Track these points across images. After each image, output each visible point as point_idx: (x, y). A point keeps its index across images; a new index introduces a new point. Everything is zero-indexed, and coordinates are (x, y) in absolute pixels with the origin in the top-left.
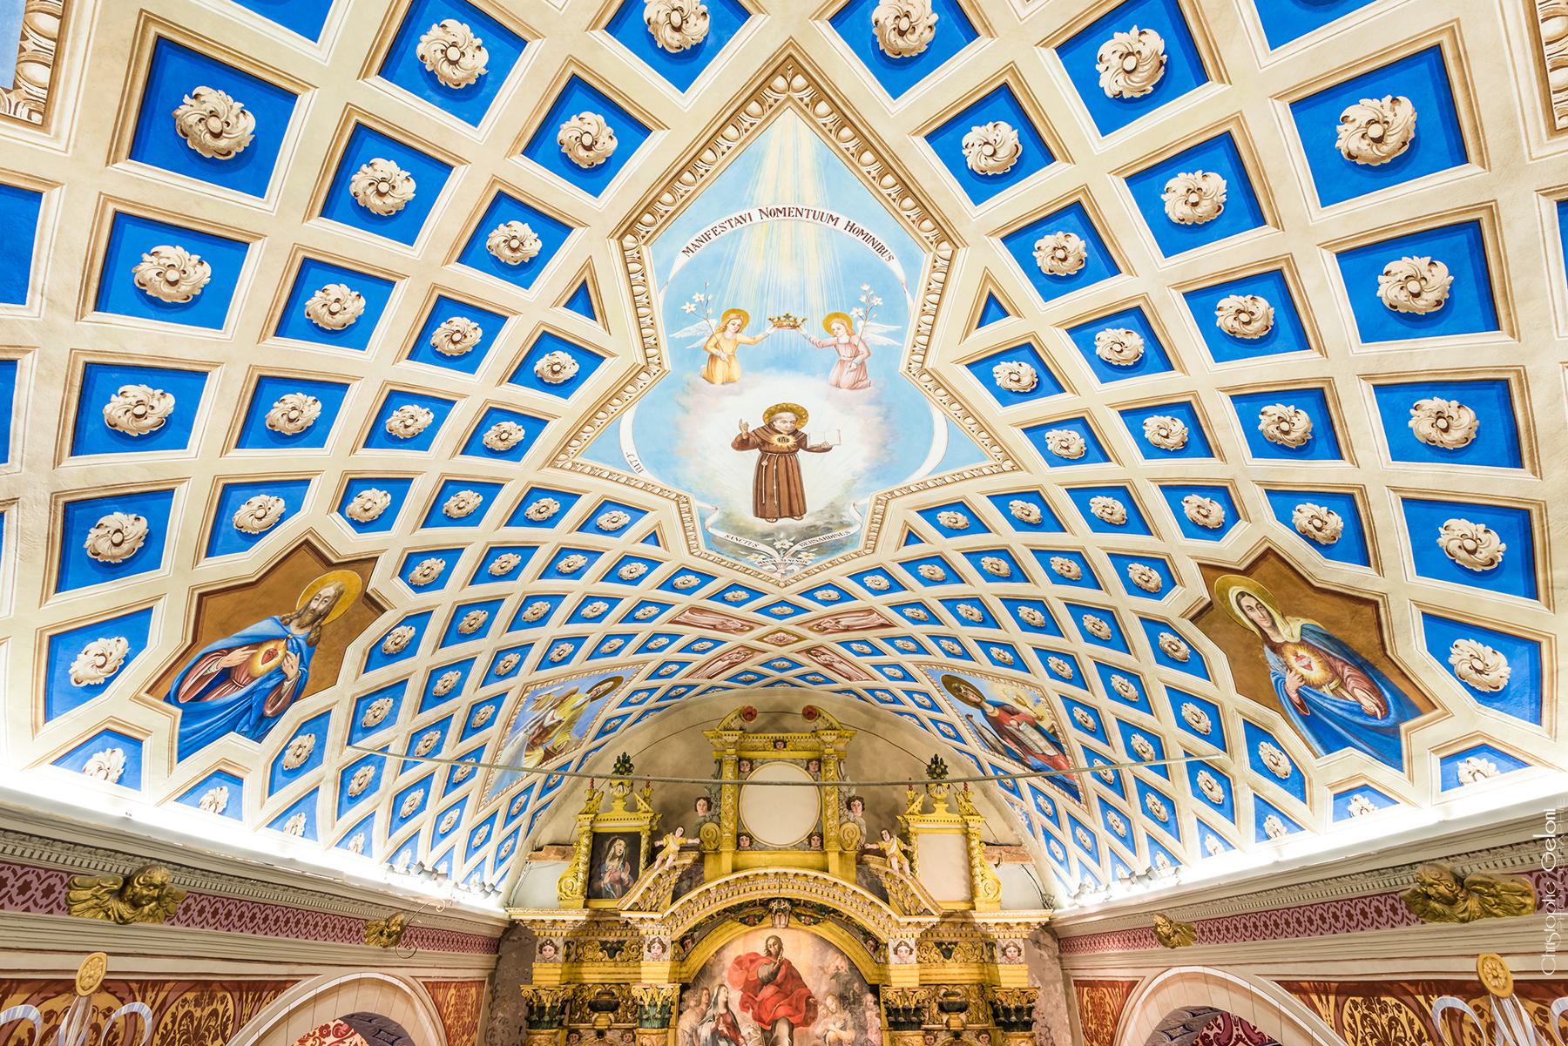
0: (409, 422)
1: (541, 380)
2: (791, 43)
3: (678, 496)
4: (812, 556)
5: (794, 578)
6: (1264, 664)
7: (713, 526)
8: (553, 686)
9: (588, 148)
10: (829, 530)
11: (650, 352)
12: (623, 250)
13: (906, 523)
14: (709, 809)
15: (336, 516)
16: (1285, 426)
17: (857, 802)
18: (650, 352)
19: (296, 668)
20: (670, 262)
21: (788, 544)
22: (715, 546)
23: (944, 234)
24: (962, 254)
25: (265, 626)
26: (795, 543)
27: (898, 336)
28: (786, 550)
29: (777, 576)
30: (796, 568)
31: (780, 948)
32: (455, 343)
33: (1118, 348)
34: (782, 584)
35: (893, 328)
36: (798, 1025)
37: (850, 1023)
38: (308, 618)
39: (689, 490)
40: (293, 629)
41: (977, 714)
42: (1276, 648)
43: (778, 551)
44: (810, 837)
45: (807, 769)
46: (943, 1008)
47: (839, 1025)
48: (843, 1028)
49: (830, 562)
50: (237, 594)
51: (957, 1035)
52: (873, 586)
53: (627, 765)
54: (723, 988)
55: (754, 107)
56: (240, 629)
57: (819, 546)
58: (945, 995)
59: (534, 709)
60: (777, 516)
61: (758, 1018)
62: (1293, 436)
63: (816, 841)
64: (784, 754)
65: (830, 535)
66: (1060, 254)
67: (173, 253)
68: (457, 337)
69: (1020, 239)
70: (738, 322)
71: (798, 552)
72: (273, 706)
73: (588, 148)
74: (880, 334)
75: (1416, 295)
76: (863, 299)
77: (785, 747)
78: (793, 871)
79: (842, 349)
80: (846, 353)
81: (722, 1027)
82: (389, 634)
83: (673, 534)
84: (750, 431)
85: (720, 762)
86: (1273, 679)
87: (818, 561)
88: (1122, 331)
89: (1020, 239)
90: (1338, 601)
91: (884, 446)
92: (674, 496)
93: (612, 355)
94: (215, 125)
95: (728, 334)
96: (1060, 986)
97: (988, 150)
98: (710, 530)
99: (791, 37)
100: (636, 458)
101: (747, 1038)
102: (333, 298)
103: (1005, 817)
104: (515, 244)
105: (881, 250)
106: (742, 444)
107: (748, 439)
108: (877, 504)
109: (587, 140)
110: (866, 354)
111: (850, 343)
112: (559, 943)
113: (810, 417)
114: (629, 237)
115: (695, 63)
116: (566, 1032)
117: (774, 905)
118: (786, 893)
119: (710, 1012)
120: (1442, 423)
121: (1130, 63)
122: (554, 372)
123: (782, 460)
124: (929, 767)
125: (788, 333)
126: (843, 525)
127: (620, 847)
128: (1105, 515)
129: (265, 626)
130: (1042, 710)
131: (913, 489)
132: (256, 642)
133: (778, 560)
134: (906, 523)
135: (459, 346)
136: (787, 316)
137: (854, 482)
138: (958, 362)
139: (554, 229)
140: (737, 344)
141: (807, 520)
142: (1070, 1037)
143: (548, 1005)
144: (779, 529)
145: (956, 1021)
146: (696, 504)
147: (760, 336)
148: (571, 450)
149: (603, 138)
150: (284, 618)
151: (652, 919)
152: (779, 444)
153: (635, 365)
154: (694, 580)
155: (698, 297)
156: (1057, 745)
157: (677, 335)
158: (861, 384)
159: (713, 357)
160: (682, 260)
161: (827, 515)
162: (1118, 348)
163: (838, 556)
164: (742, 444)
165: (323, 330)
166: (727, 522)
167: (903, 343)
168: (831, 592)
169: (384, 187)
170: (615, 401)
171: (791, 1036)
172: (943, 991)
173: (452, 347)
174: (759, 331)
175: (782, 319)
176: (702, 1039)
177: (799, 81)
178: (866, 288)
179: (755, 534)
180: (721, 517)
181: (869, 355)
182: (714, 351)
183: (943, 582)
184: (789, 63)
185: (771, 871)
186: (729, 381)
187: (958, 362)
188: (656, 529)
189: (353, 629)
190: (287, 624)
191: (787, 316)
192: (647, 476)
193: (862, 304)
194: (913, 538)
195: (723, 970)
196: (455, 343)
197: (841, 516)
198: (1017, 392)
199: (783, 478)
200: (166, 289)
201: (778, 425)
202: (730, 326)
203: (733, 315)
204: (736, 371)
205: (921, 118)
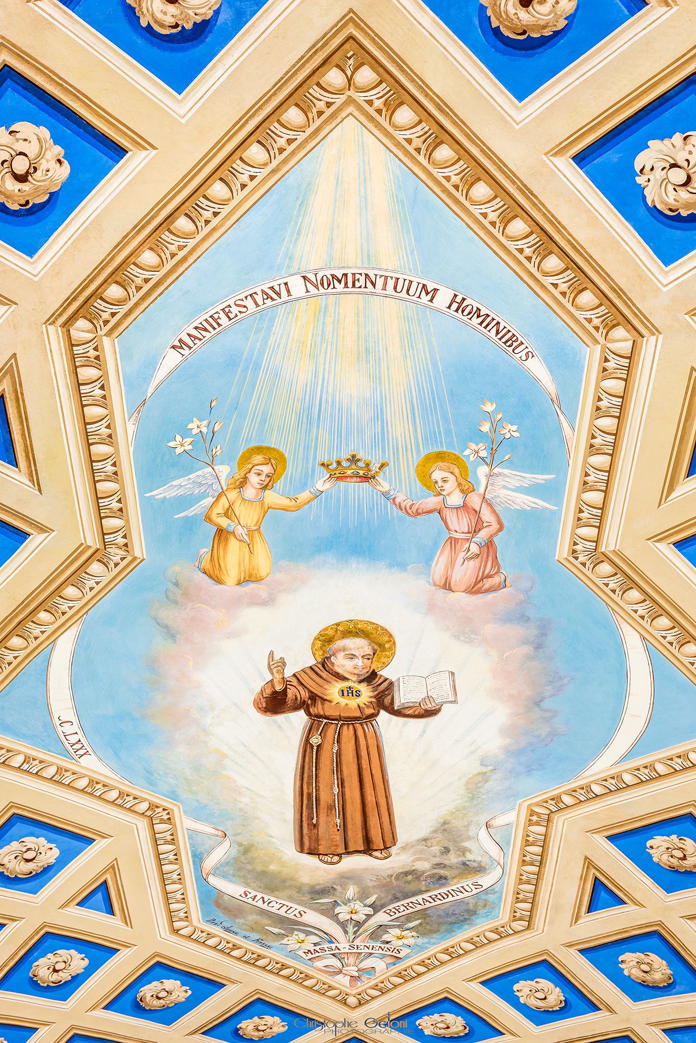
2: (351, 17)
3: (153, 807)
4: (410, 939)
5: (375, 987)
9: (22, 178)
10: (441, 880)
11: (111, 523)
13: (589, 863)
18: (111, 523)
20: (152, 364)
21: (362, 911)
22: (220, 916)
24: (650, 346)
27: (551, 491)
28: (359, 924)
29: (342, 981)
30: (380, 965)
34: (352, 1001)
35: (540, 478)
39: (174, 796)
43: (343, 925)
49: (446, 951)
52: (533, 1002)
55: (293, 115)
60: (341, 850)
65: (443, 890)
70: (267, 469)
73: (22, 178)
74: (518, 490)
76: (486, 428)
79: (452, 518)
80: (460, 524)
84: (288, 673)
87: (422, 948)
91: (537, 704)
92: (143, 807)
93: (42, 529)
95: (250, 492)
98: (212, 880)
99: (351, 11)
100: (75, 728)
105: (511, 341)
107: (285, 690)
108: (530, 823)
109: (20, 166)
110: (495, 526)
111: (465, 506)
114: (82, 323)
115: (199, 50)
123: (348, 733)
125: (354, 488)
126: (469, 869)
131: (597, 789)
133: (344, 946)
134: (589, 863)
136: (354, 459)
137: (484, 777)
138: (659, 538)
140: (266, 510)
144: (346, 878)
146: (185, 823)
147: (304, 496)
149: (48, 163)
152: (343, 701)
153: (81, 548)
154: (178, 991)
157: (159, 493)
158: (488, 583)
159: (221, 534)
160: (173, 359)
161: (436, 849)
163: (461, 936)
167: (559, 504)
168: (450, 1018)
170: (43, 616)
174: (304, 486)
175: (345, 464)
178: (489, 407)
179: (299, 889)
180: (234, 852)
181: (501, 527)
182: (224, 522)
183: (667, 989)
186: (249, 578)
187: (659, 538)
188: (108, 877)
191: (354, 459)
192: (92, 764)
193: (482, 436)
194: (603, 894)
197: (464, 851)
199: (350, 770)
201: (341, 663)
202: (254, 479)
203: (258, 459)
204: (263, 561)
205: (563, 128)
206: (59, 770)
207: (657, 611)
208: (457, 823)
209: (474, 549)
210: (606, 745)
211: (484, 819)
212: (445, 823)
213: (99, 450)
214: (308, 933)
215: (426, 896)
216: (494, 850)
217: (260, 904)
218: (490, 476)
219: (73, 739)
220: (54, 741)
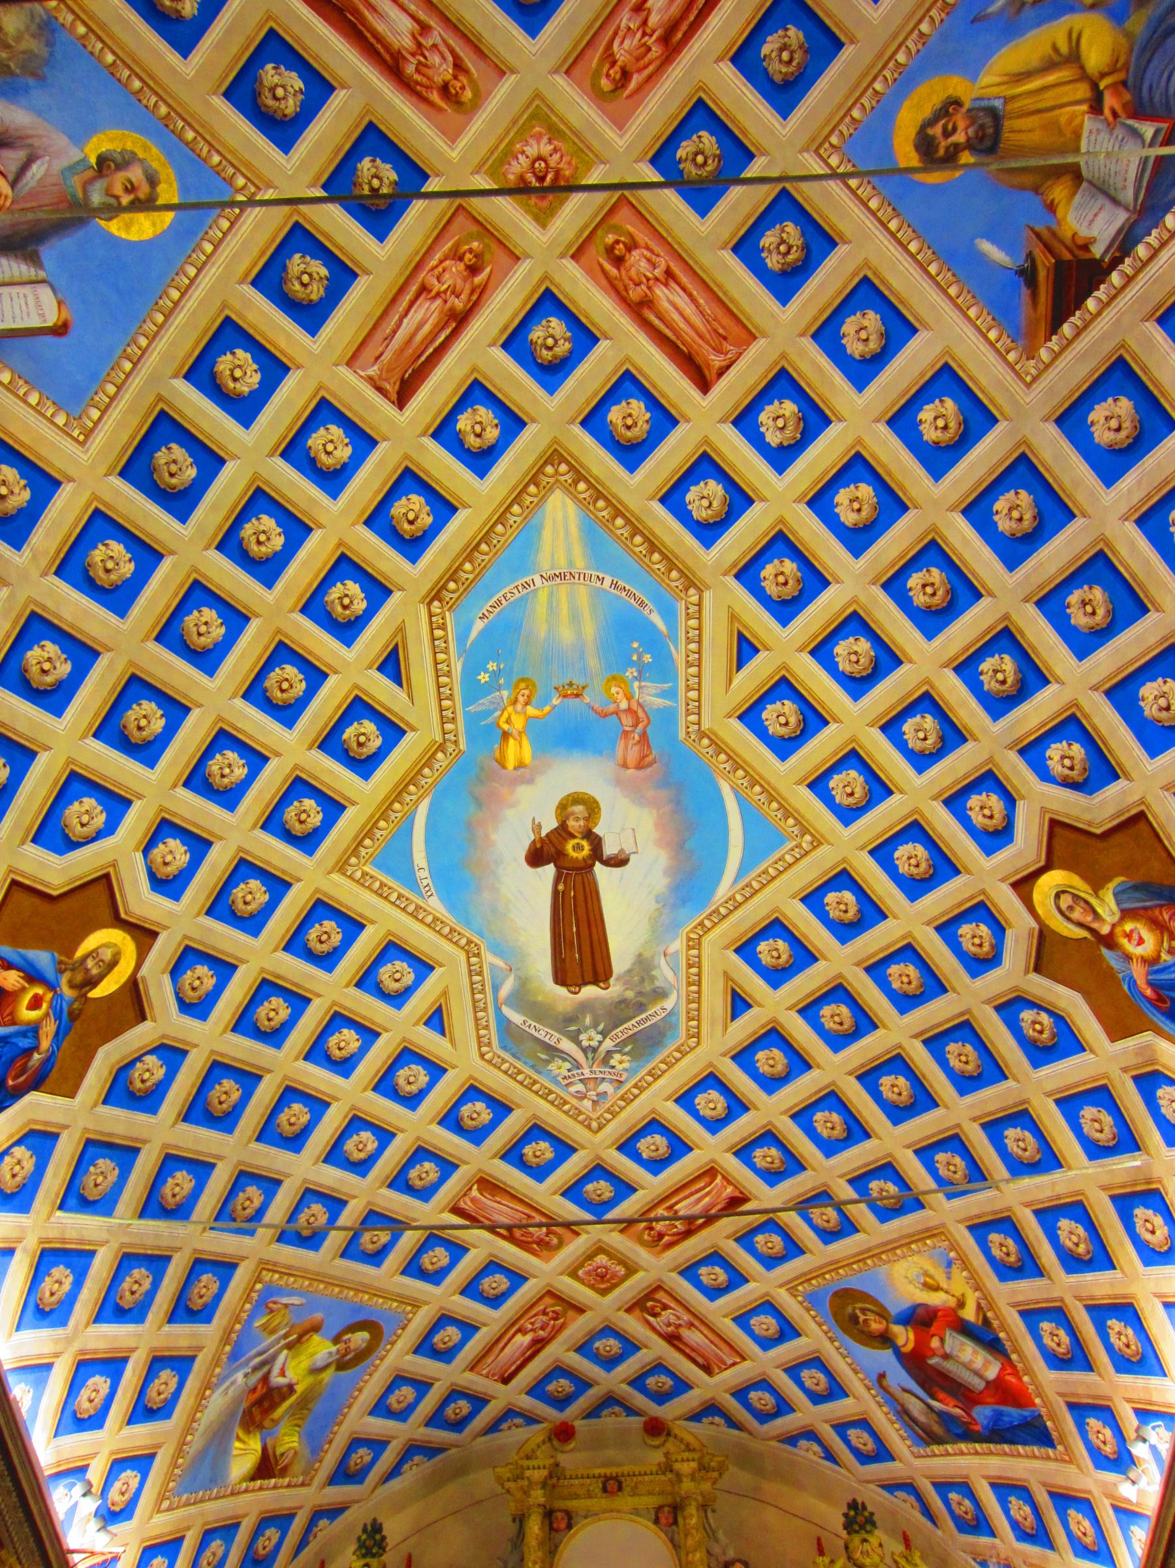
0: (227, 771)
1: (347, 751)
2: (555, 441)
3: (469, 942)
6: (1110, 975)
7: (509, 1001)
9: (411, 523)
10: (641, 1007)
12: (431, 615)
15: (139, 855)
16: (1000, 676)
18: (448, 726)
19: (50, 1038)
23: (690, 582)
24: (707, 595)
25: (42, 958)
26: (604, 1034)
27: (671, 694)
32: (282, 691)
33: (854, 658)
38: (79, 978)
39: (481, 935)
40: (64, 980)
41: (885, 1358)
42: (1109, 941)
43: (585, 1050)
45: (656, 1521)
50: (37, 901)
53: (378, 1537)
55: (532, 489)
56: (25, 947)
57: (632, 1038)
62: (1010, 681)
65: (643, 1016)
66: (781, 579)
67: (117, 548)
68: (285, 685)
69: (747, 573)
70: (526, 692)
71: (609, 1054)
72: (14, 1079)
73: (411, 523)
75: (1020, 520)
76: (635, 658)
77: (620, 1489)
79: (623, 717)
80: (627, 721)
82: (139, 1059)
83: (460, 1017)
84: (543, 834)
85: (520, 1519)
86: (1126, 987)
88: (851, 639)
89: (747, 573)
90: (1119, 838)
94: (174, 468)
95: (519, 707)
97: (705, 503)
98: (506, 1011)
102: (204, 619)
104: (346, 601)
106: (536, 857)
109: (411, 516)
113: (598, 798)
114: (436, 603)
115: (491, 458)
120: (1089, 609)
121: (780, 423)
122: (360, 745)
128: (914, 870)
129: (42, 958)
130: (959, 1284)
132: (33, 976)
135: (285, 695)
136: (571, 684)
139: (378, 591)
140: (528, 718)
141: (615, 990)
144: (584, 1007)
146: (489, 958)
147: (547, 708)
148: (363, 852)
149: (423, 515)
150: (61, 962)
155: (492, 666)
159: (506, 735)
160: (479, 625)
162: (854, 658)
164: (536, 857)
165: (188, 647)
166: (523, 999)
169: (263, 538)
173: (279, 694)
177: (563, 468)
178: (635, 645)
182: (506, 727)
184: (555, 456)
189: (112, 1032)
190: (61, 972)
191: (571, 684)
196: (282, 691)
198: (790, 739)
200: (101, 573)
201: (572, 824)
202: (521, 699)
203: (523, 685)
206: (418, 907)
207: (737, 767)
208: (647, 954)
209: (637, 737)
210: (721, 873)
211: (661, 949)
212: (640, 955)
213: (443, 680)
214: (564, 1060)
215: (633, 1022)
216: (670, 975)
217: (533, 1031)
218: (640, 688)
219: (425, 882)
220: (413, 884)
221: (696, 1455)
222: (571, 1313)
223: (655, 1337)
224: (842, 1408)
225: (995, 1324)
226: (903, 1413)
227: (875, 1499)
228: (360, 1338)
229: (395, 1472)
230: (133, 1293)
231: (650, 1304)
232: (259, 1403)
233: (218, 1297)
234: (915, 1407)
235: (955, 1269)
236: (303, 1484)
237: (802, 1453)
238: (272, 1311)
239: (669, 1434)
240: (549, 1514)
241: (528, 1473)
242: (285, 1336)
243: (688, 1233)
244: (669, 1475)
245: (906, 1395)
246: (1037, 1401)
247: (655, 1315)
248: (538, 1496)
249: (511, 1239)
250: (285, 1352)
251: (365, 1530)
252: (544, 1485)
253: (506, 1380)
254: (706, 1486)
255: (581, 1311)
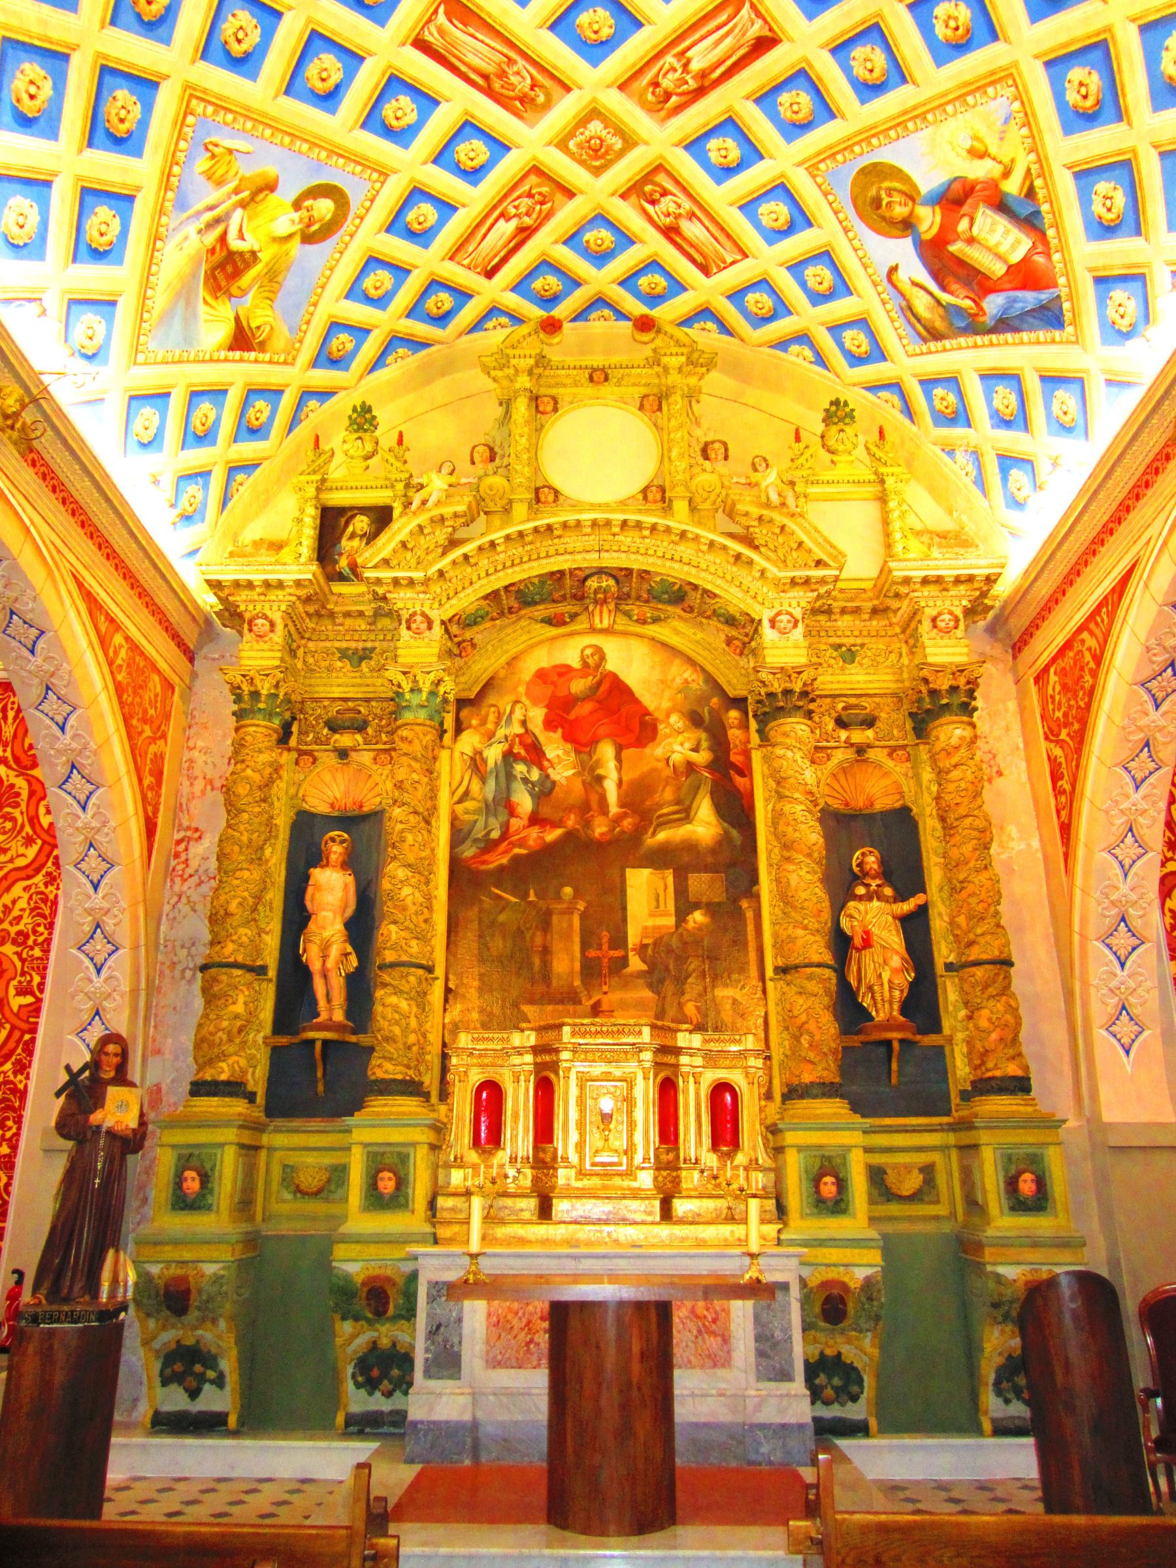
8: (236, 133)
14: (492, 459)
17: (717, 445)
31: (603, 658)
36: (629, 746)
37: (705, 744)
44: (645, 491)
46: (841, 723)
47: (687, 745)
48: (696, 749)
51: (861, 750)
54: (518, 706)
58: (844, 709)
59: (209, 175)
61: (566, 738)
63: (654, 494)
64: (606, 390)
77: (606, 379)
78: (618, 517)
81: (517, 749)
85: (507, 404)
96: (1012, 705)
101: (555, 761)
103: (938, 491)
112: (277, 617)
116: (294, 755)
117: (592, 583)
118: (611, 560)
119: (501, 733)
124: (827, 411)
127: (361, 523)
142: (1023, 765)
143: (264, 692)
145: (860, 736)
151: (411, 582)
156: (1031, 222)
171: (618, 758)
172: (840, 706)
176: (491, 763)
185: (587, 517)
195: (519, 683)
221: (685, 350)
222: (559, 197)
223: (651, 230)
224: (841, 309)
225: (1041, 194)
226: (908, 310)
227: (857, 399)
228: (324, 208)
229: (378, 363)
230: (32, 97)
231: (648, 188)
232: (221, 266)
233: (144, 123)
234: (921, 303)
235: (1013, 126)
236: (285, 363)
237: (793, 359)
238: (213, 156)
239: (659, 331)
240: (535, 399)
241: (513, 362)
242: (237, 192)
243: (700, 92)
244: (656, 369)
245: (916, 289)
246: (1062, 281)
247: (653, 202)
248: (524, 381)
249: (489, 92)
250: (239, 211)
251: (355, 409)
252: (530, 373)
253: (490, 274)
254: (693, 381)
255: (570, 194)
